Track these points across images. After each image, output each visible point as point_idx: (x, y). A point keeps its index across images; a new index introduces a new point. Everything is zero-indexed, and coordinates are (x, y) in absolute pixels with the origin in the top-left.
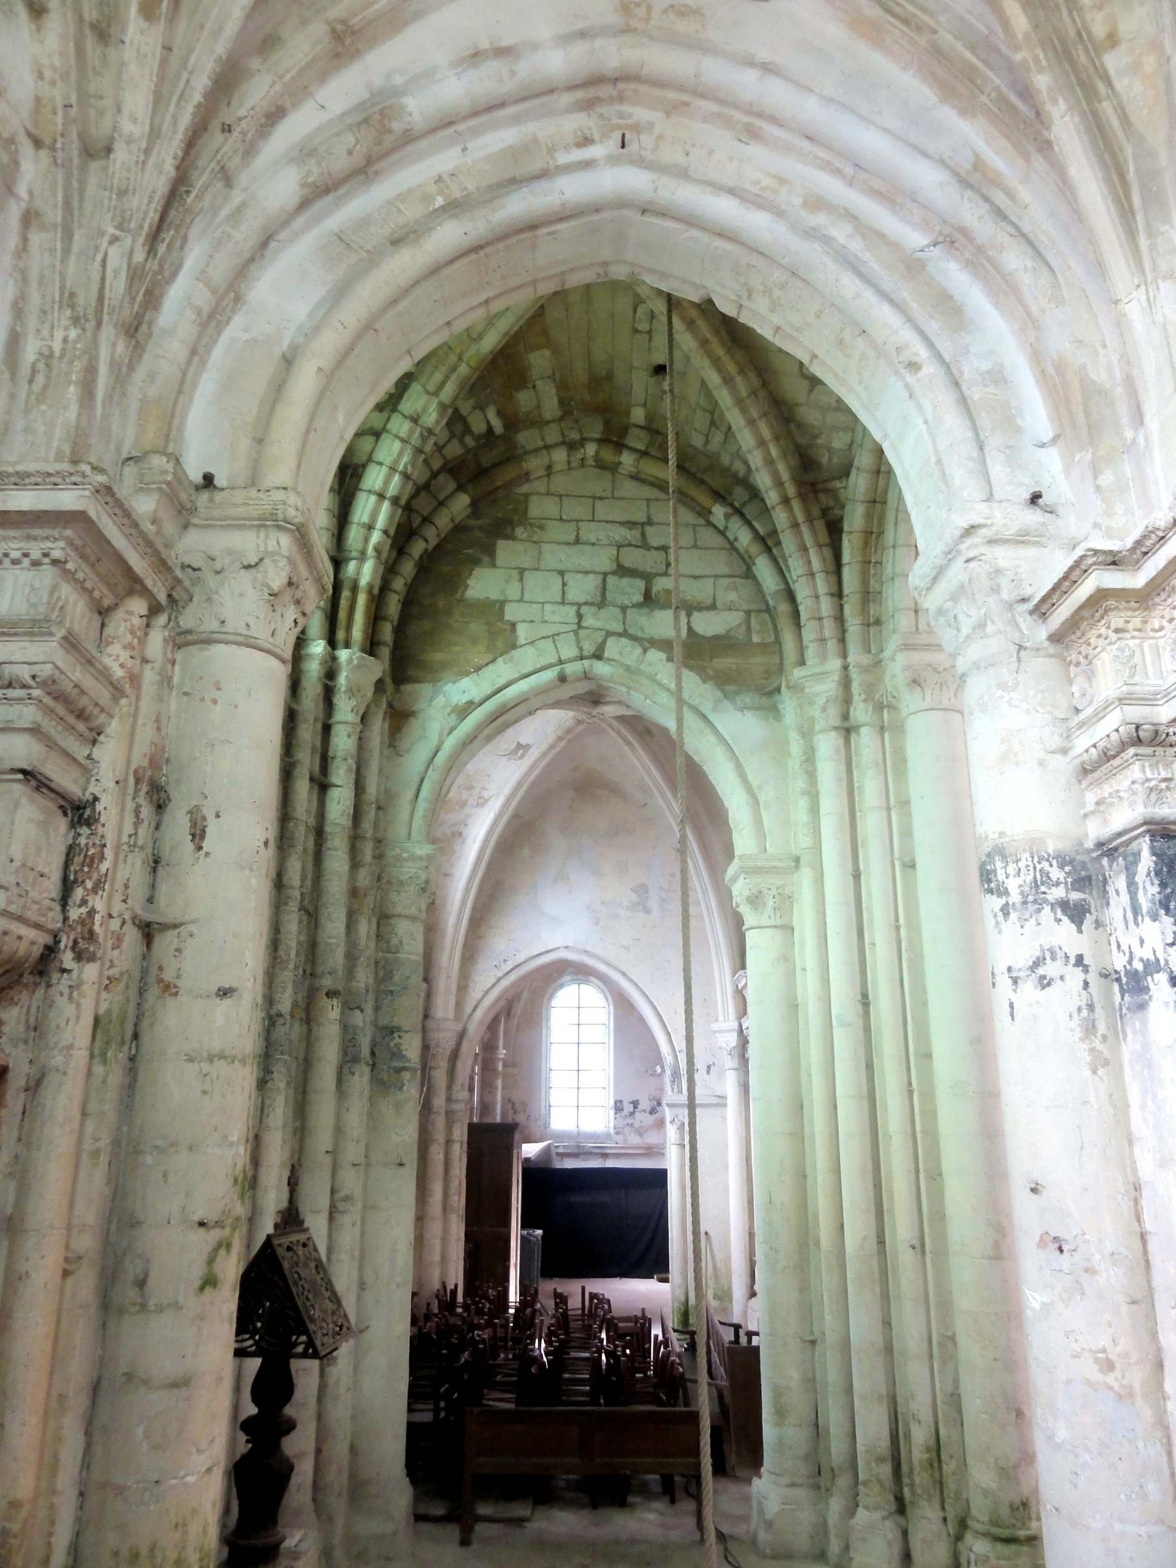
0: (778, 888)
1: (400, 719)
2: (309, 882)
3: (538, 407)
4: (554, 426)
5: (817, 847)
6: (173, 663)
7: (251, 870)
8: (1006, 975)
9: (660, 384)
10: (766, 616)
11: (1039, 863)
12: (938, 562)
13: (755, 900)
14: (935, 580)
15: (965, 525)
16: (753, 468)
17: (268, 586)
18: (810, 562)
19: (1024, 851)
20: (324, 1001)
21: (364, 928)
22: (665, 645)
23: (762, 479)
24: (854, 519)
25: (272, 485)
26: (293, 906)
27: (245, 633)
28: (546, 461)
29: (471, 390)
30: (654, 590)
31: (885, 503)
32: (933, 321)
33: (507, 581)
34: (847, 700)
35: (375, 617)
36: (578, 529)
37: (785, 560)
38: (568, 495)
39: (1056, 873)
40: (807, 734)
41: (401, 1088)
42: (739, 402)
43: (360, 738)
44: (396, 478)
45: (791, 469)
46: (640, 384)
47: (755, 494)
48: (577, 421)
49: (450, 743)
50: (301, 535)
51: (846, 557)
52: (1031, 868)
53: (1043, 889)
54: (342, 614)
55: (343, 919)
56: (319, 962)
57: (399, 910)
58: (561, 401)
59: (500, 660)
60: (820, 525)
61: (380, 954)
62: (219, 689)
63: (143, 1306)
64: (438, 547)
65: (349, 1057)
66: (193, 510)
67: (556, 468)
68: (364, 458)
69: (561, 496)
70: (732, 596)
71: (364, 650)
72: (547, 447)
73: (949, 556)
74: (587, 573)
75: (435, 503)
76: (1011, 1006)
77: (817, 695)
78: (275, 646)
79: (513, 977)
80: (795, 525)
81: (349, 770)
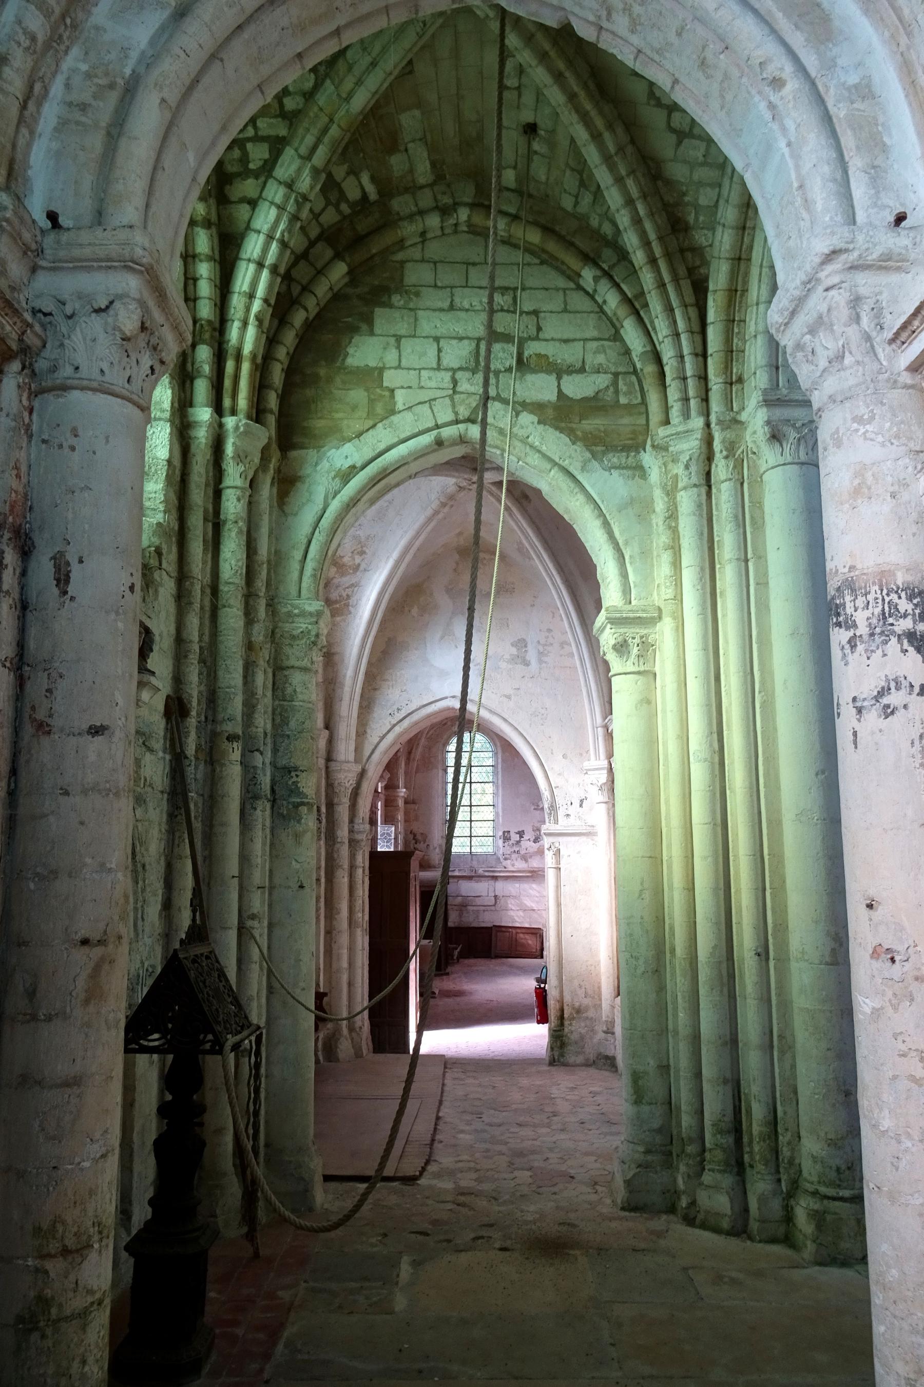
0: (642, 637)
1: (287, 484)
2: (206, 638)
3: (411, 171)
4: (428, 192)
5: (678, 598)
6: (31, 412)
7: (117, 613)
8: (851, 705)
10: (634, 378)
11: (888, 595)
12: (797, 293)
13: (621, 648)
14: (793, 313)
15: (827, 251)
16: (621, 228)
17: (121, 330)
18: (675, 322)
19: (874, 583)
20: (226, 745)
21: (261, 679)
22: (537, 408)
23: (631, 240)
24: (719, 278)
25: (118, 224)
26: (194, 658)
27: (100, 378)
28: (420, 228)
29: (344, 153)
30: (526, 354)
31: (749, 260)
32: (798, 33)
33: (385, 348)
34: (710, 458)
35: (260, 387)
36: (452, 295)
37: (652, 322)
38: (442, 262)
39: (904, 605)
40: (671, 492)
41: (299, 822)
42: (607, 159)
43: (250, 503)
44: (274, 246)
45: (658, 228)
47: (623, 256)
48: (449, 186)
49: (335, 505)
50: (152, 277)
51: (711, 316)
52: (880, 601)
53: (891, 620)
54: (228, 383)
55: (240, 670)
56: (220, 709)
57: (292, 662)
58: (433, 164)
59: (380, 425)
60: (686, 285)
61: (277, 702)
62: (76, 436)
63: (34, 1018)
64: (318, 315)
65: (250, 796)
66: (39, 252)
67: (429, 236)
68: (243, 226)
69: (435, 263)
70: (600, 359)
71: (249, 417)
72: (421, 213)
73: (809, 286)
74: (461, 339)
75: (314, 272)
76: (855, 734)
77: (682, 452)
78: (132, 393)
79: (406, 723)
80: (662, 285)
81: (240, 532)
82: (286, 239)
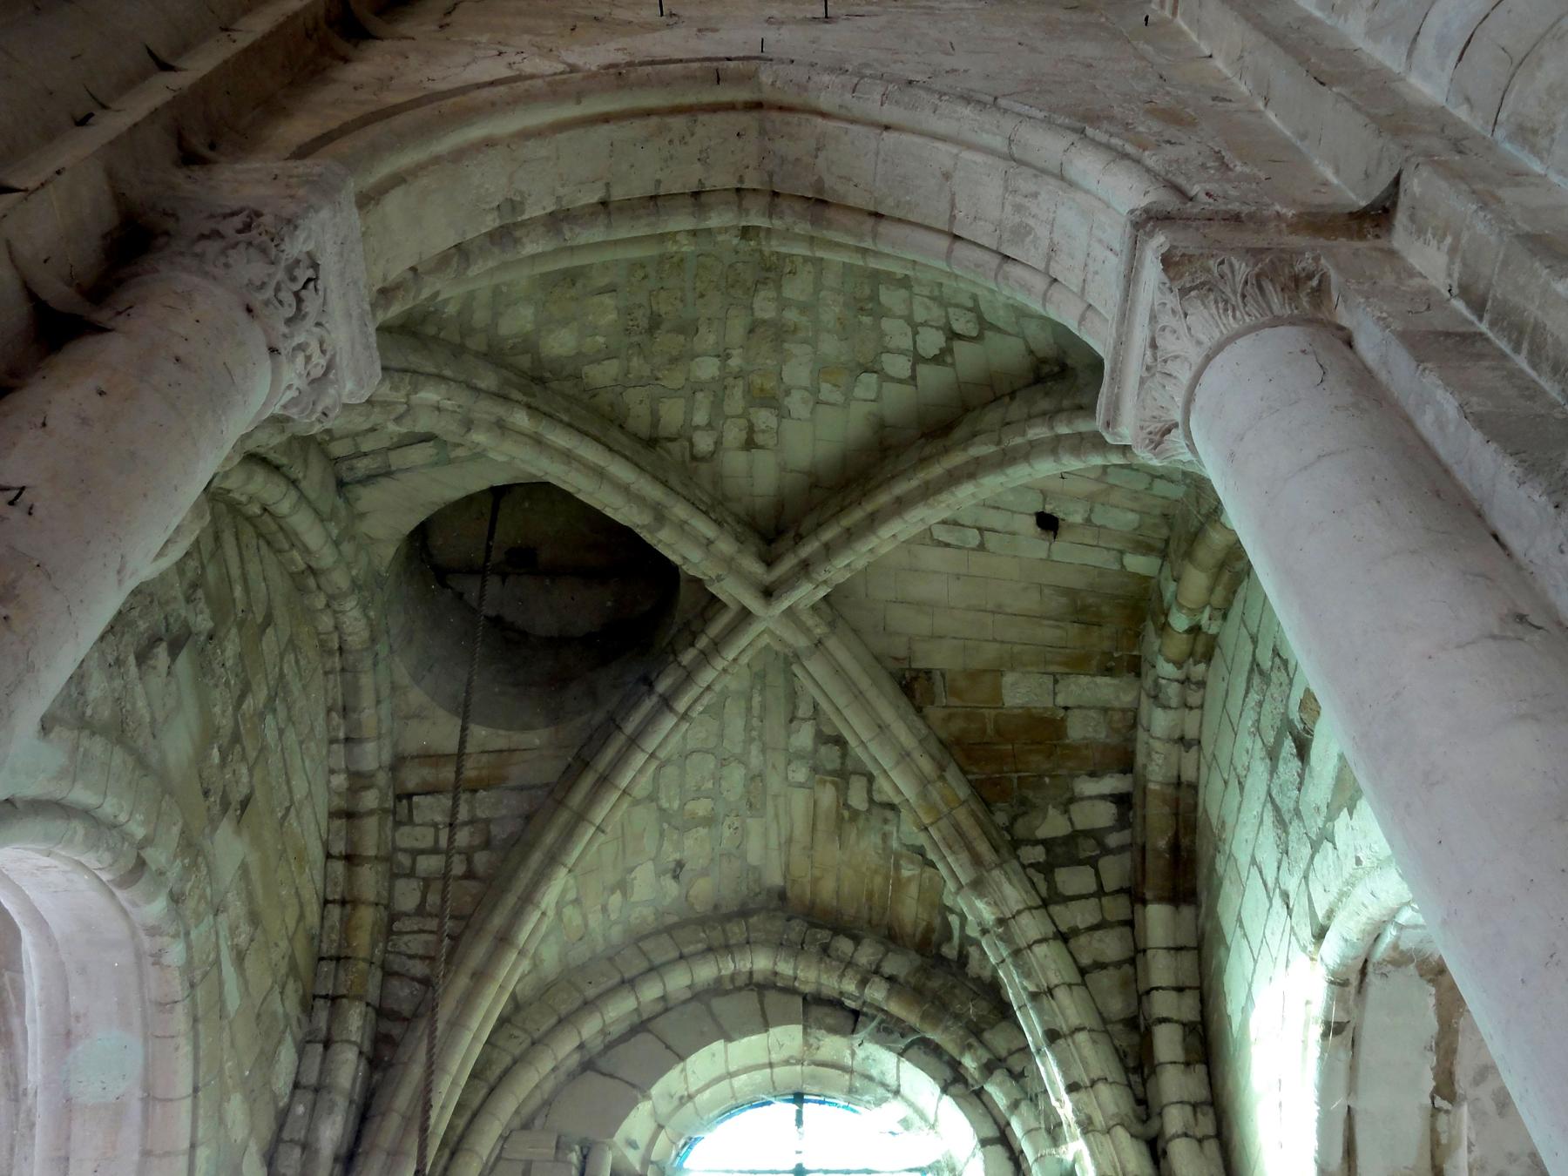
3: (1105, 710)
9: (1072, 526)
46: (1075, 557)
58: (1108, 671)
67: (1191, 733)
82: (1032, 988)
